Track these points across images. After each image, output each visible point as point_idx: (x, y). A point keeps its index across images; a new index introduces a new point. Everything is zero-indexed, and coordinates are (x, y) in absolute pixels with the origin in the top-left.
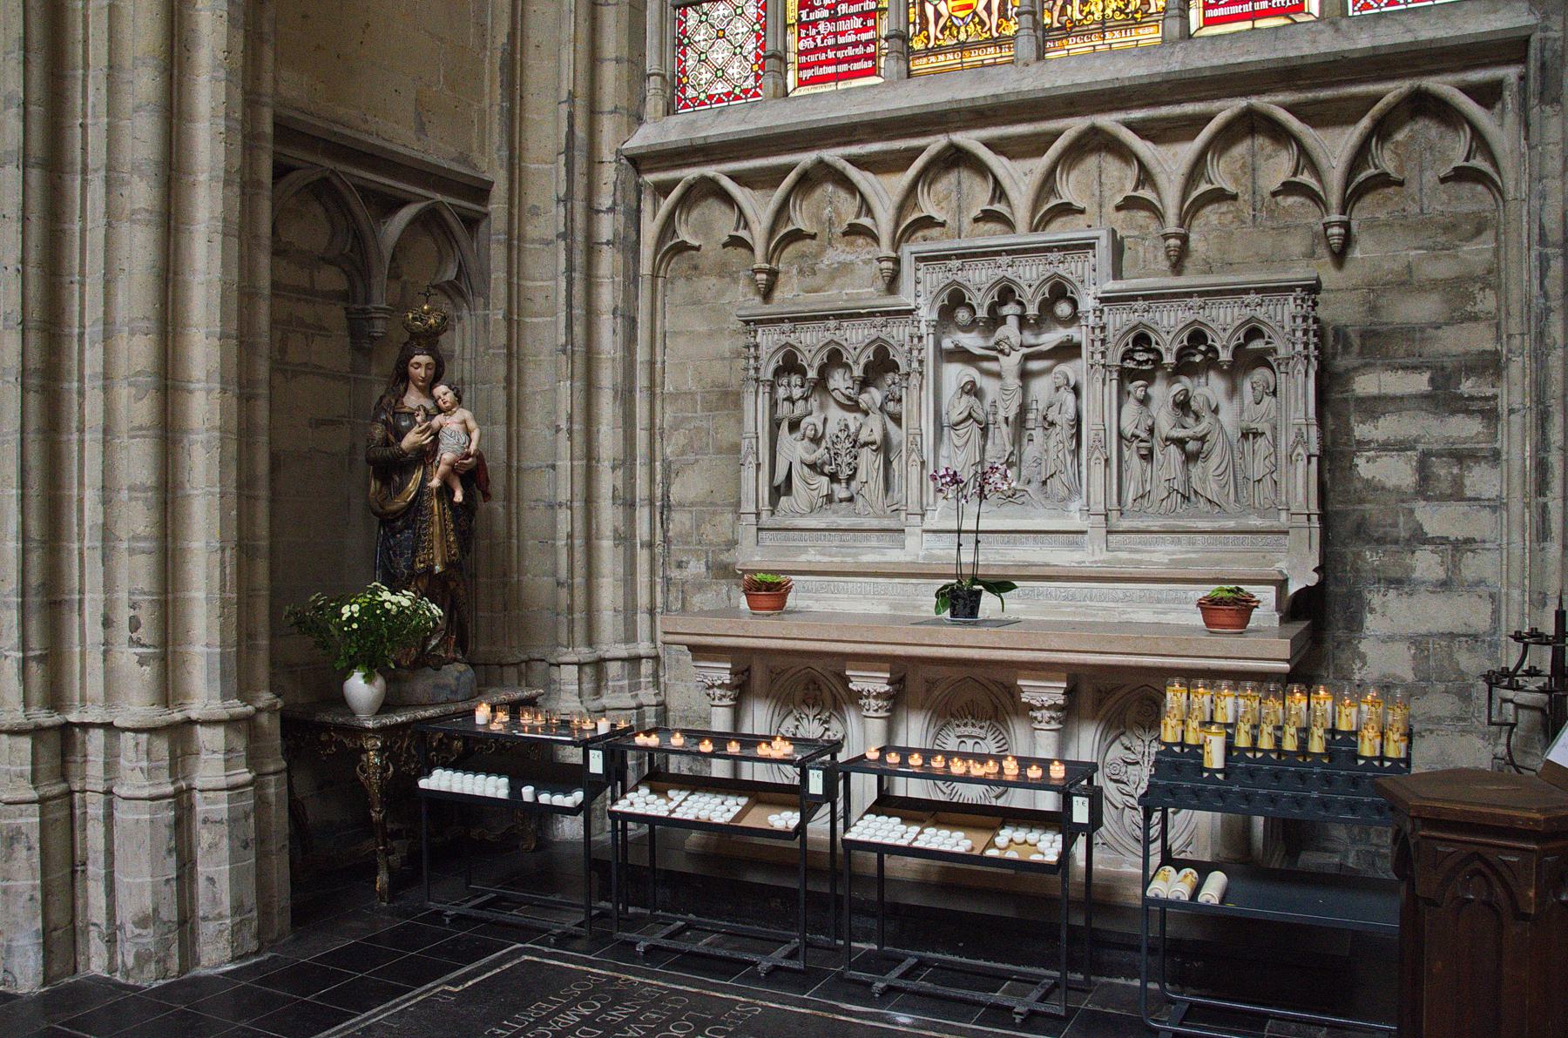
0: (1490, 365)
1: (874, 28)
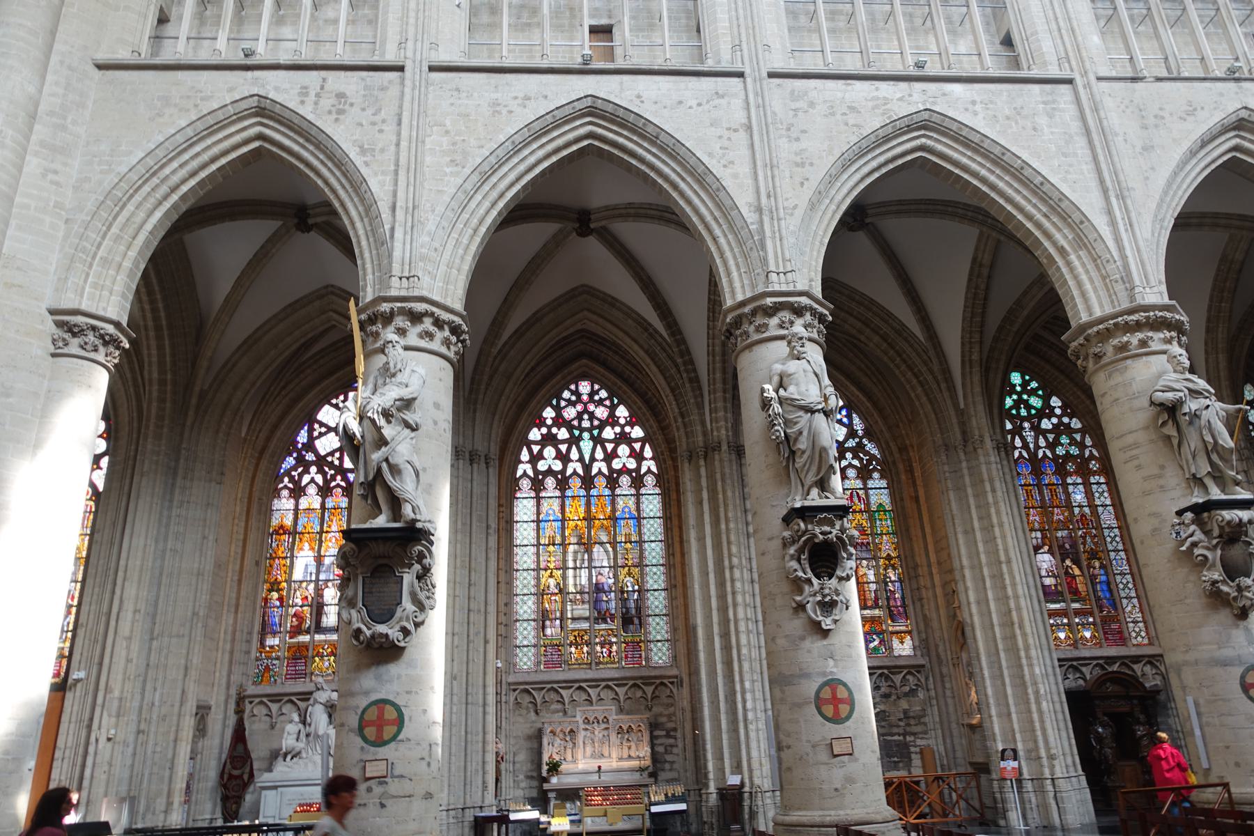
0: (675, 730)
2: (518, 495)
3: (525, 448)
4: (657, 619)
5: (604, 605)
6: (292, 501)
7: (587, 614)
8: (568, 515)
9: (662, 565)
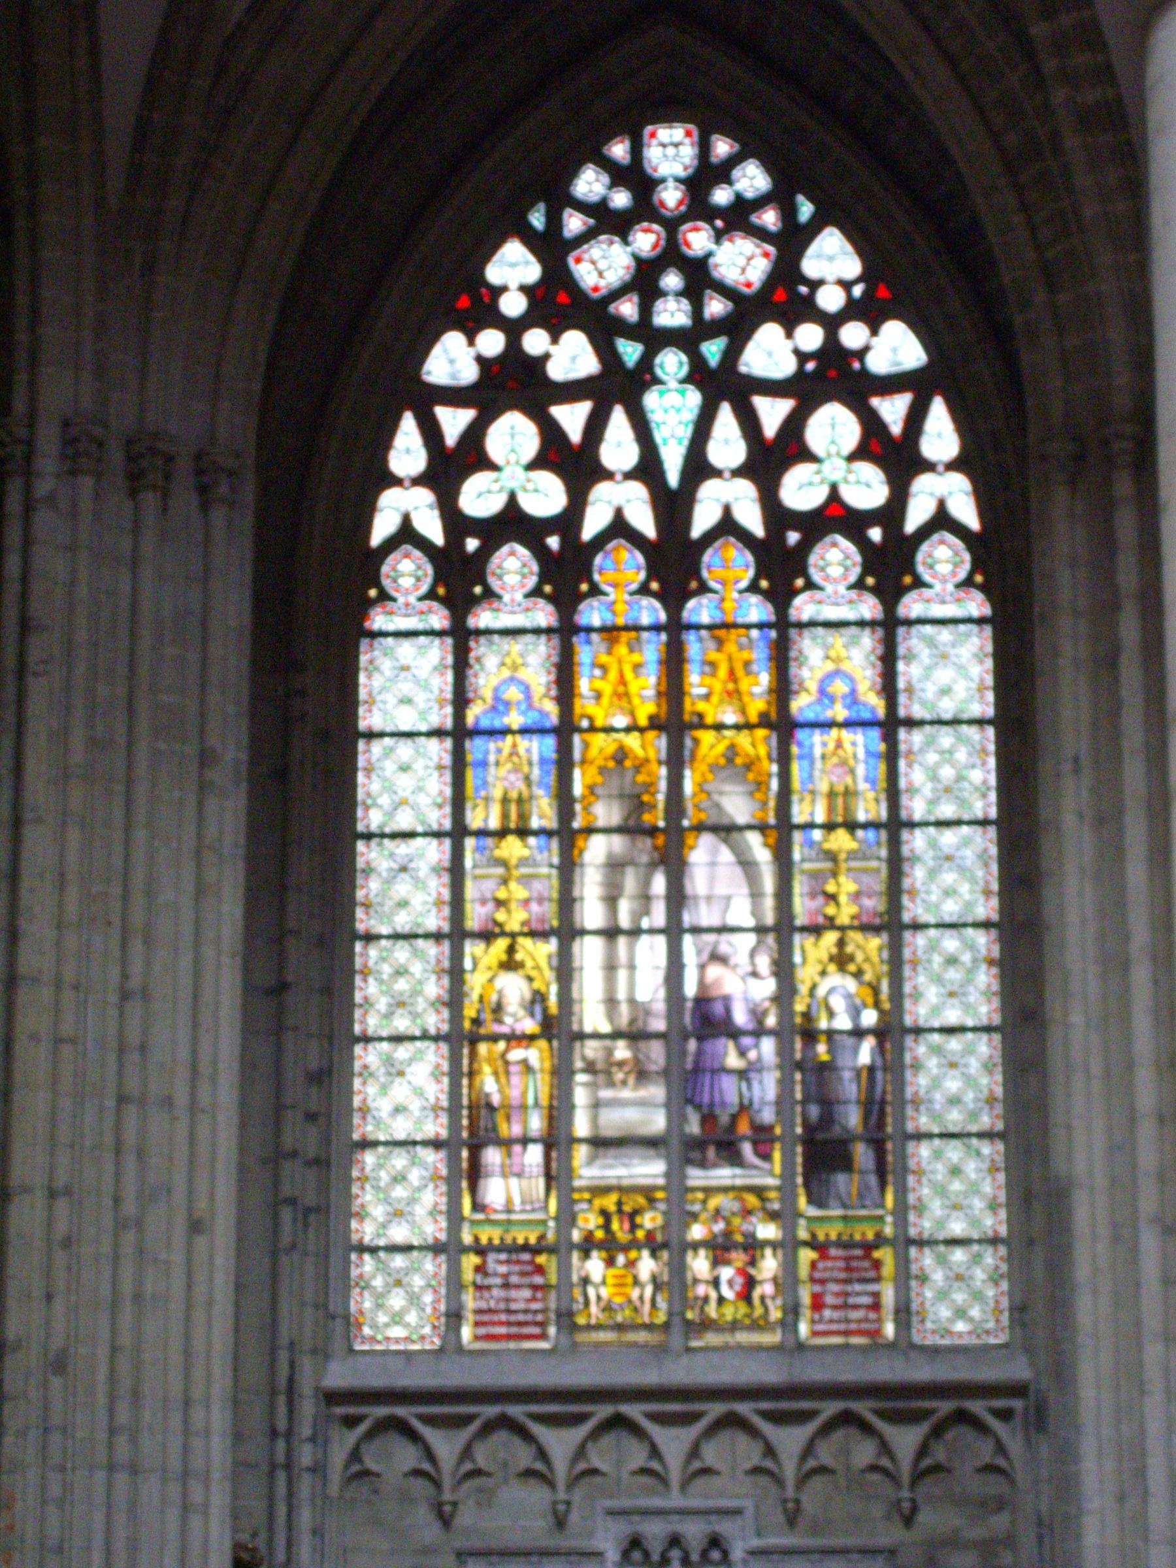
1: (544, 1300)
2: (379, 620)
3: (408, 425)
4: (954, 1152)
5: (730, 1089)
7: (658, 1122)
8: (584, 706)
9: (986, 925)
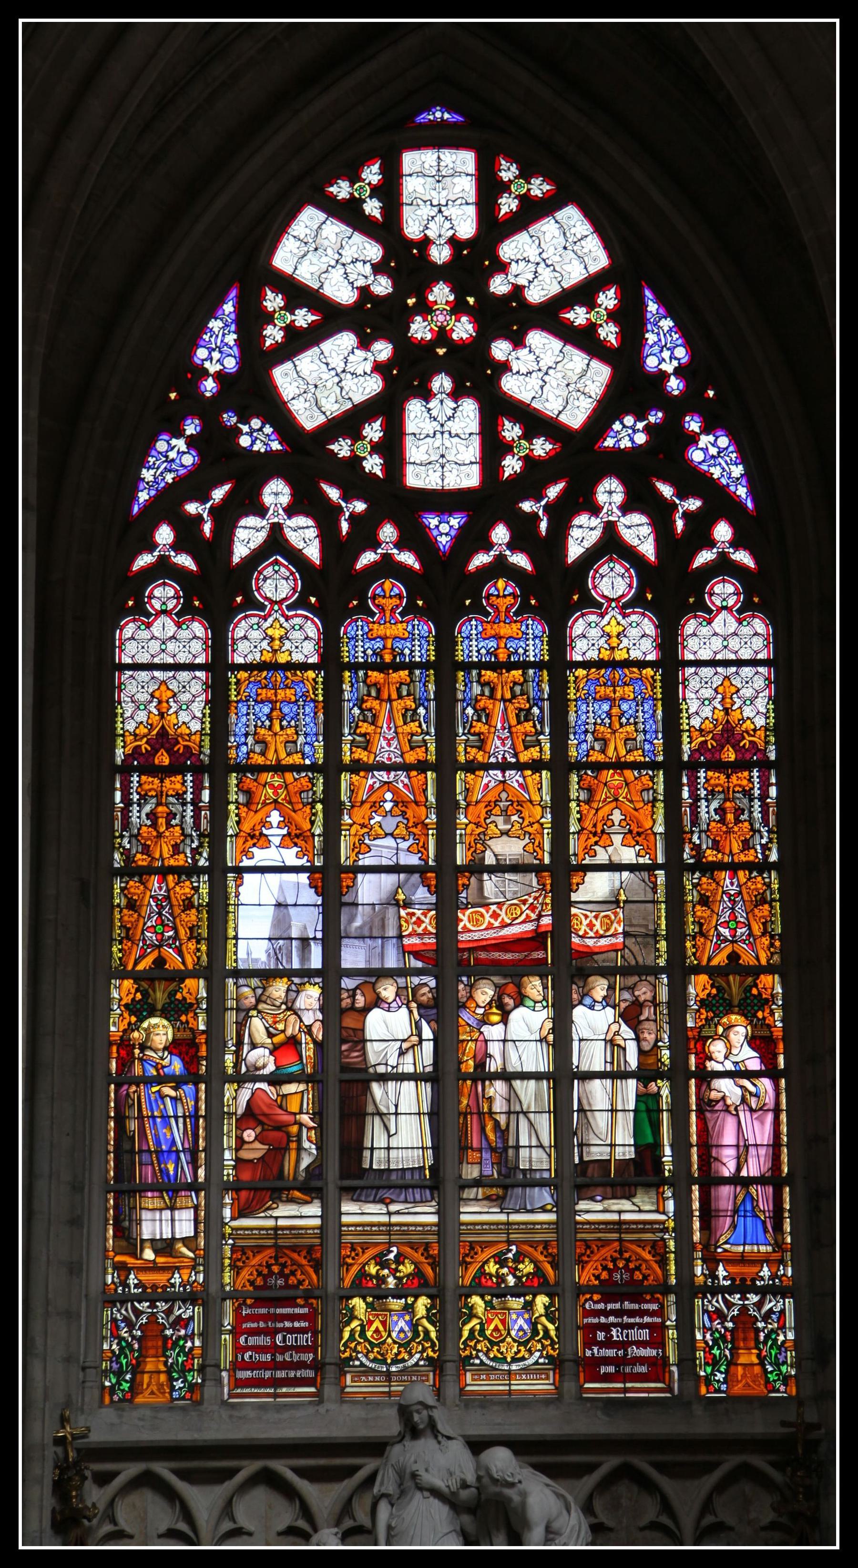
6: (198, 628)
